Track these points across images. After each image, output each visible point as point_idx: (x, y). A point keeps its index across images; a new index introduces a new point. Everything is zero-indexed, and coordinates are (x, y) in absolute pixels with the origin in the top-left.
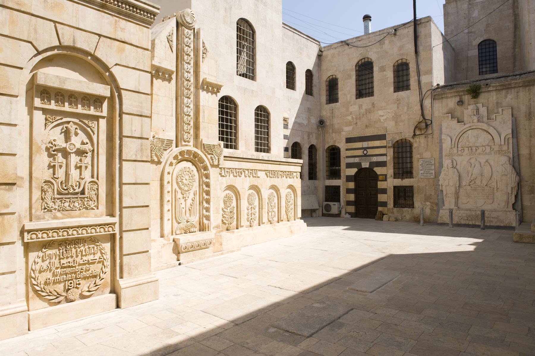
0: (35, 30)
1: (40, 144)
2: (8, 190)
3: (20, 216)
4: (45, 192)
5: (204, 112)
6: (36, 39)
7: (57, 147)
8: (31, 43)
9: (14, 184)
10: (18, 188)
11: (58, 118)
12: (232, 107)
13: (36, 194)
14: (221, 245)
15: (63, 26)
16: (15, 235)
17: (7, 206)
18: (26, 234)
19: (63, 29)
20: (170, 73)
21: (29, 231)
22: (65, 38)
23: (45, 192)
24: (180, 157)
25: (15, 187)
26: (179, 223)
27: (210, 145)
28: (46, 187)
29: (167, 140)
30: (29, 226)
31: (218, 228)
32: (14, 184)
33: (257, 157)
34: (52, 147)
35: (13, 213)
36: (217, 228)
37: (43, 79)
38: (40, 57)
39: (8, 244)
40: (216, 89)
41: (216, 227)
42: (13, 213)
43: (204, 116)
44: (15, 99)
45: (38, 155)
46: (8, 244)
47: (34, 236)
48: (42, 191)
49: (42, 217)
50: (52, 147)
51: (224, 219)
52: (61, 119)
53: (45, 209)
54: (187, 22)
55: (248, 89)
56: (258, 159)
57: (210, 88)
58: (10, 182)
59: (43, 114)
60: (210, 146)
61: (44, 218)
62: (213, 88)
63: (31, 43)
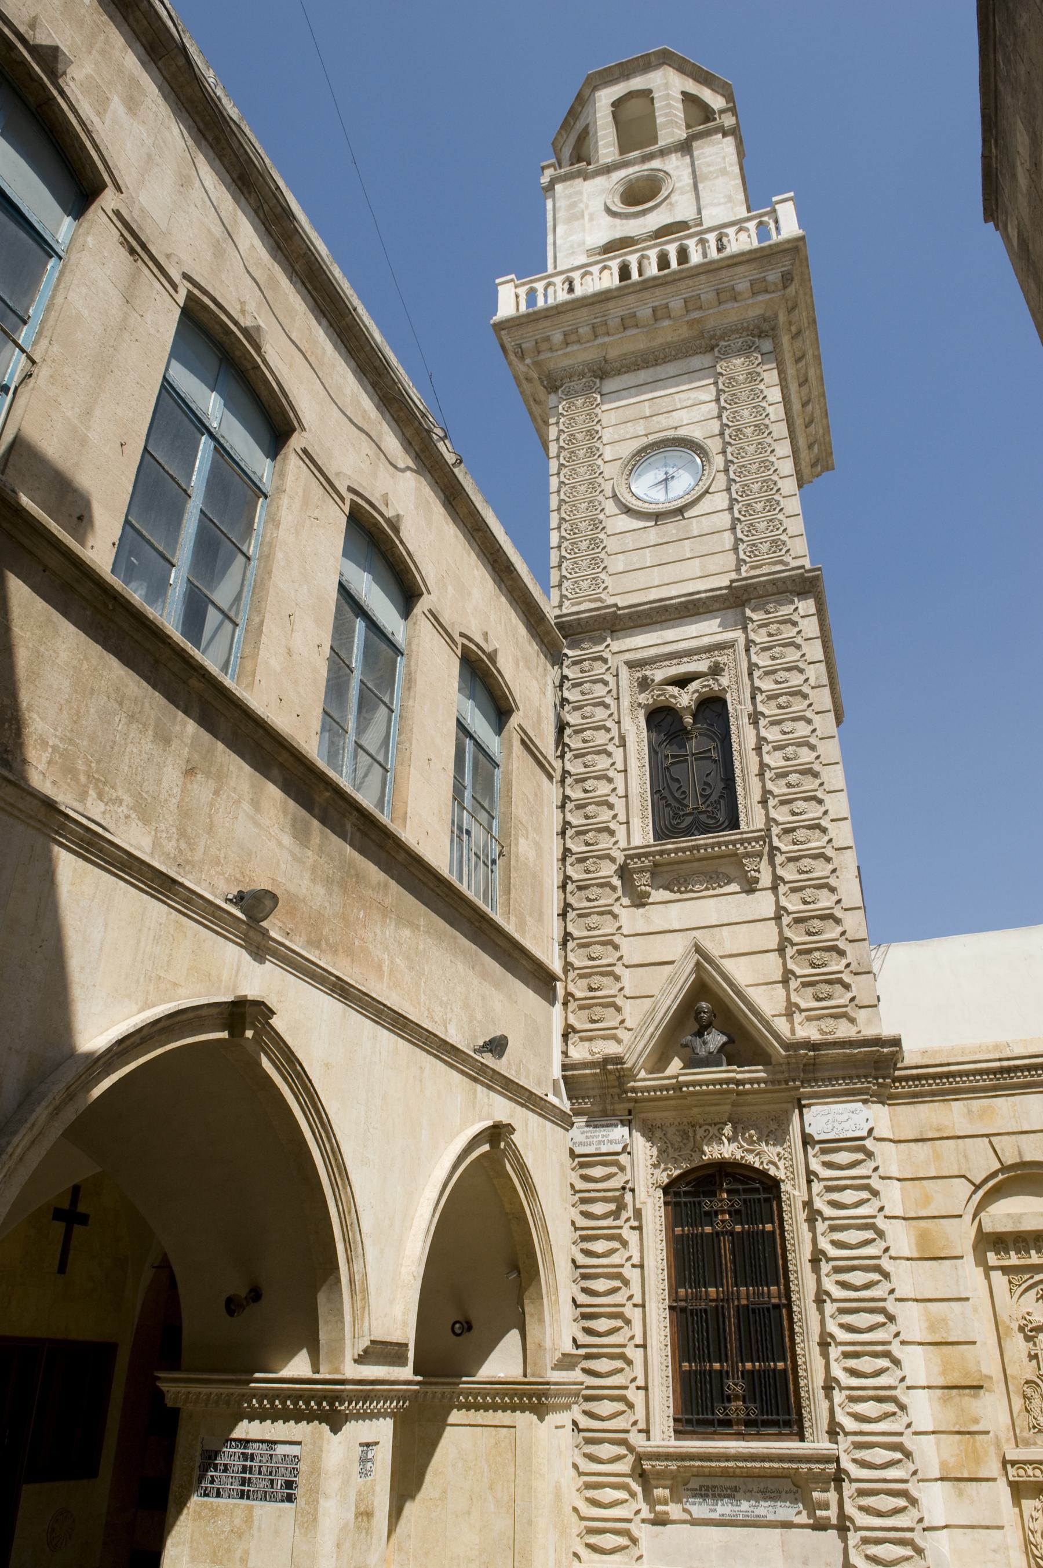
0: (966, 1157)
1: (1008, 1322)
2: (975, 1396)
3: (997, 1437)
4: (1029, 1399)
6: (969, 1170)
7: (1034, 1325)
8: (964, 1176)
9: (981, 1387)
10: (987, 1394)
11: (1026, 1277)
13: (1018, 1403)
15: (999, 1138)
16: (993, 1468)
17: (976, 1421)
18: (1009, 1466)
19: (1000, 1141)
21: (1013, 1463)
22: (1007, 1154)
23: (1029, 1399)
25: (982, 1392)
28: (1029, 1392)
30: (1012, 1454)
32: (981, 1387)
34: (1027, 1325)
35: (987, 1433)
37: (990, 1224)
38: (981, 1193)
39: (988, 1480)
42: (987, 1433)
44: (960, 1261)
45: (1008, 1339)
46: (988, 1480)
47: (1021, 1472)
48: (1025, 1397)
49: (1032, 1442)
50: (1027, 1325)
52: (1032, 1277)
53: (1034, 1427)
58: (975, 1384)
59: (1004, 1274)
61: (1035, 1444)
63: (964, 1176)
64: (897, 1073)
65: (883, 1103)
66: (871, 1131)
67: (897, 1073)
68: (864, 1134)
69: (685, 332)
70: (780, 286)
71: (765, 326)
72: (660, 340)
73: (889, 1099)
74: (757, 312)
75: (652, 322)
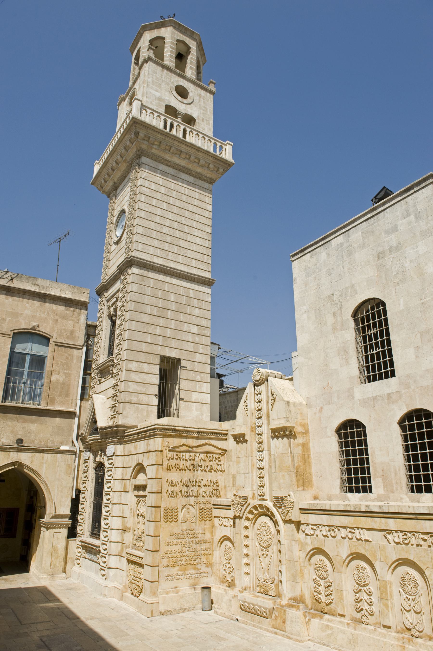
5: (275, 461)
12: (360, 431)
14: (284, 622)
20: (243, 435)
24: (255, 512)
26: (259, 581)
27: (278, 497)
29: (243, 496)
31: (296, 602)
32: (126, 531)
33: (355, 508)
35: (125, 544)
36: (294, 602)
40: (282, 432)
41: (293, 600)
42: (125, 544)
43: (275, 465)
51: (315, 594)
54: (256, 381)
55: (379, 396)
56: (357, 510)
57: (277, 434)
59: (136, 497)
60: (279, 499)
62: (279, 433)
64: (125, 434)
65: (121, 444)
66: (114, 453)
67: (125, 434)
68: (112, 455)
69: (125, 165)
70: (136, 138)
71: (140, 153)
72: (122, 171)
73: (124, 442)
74: (135, 150)
75: (117, 166)
